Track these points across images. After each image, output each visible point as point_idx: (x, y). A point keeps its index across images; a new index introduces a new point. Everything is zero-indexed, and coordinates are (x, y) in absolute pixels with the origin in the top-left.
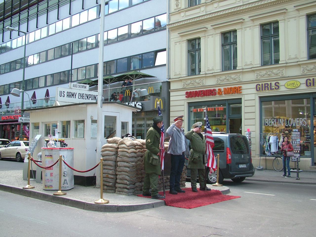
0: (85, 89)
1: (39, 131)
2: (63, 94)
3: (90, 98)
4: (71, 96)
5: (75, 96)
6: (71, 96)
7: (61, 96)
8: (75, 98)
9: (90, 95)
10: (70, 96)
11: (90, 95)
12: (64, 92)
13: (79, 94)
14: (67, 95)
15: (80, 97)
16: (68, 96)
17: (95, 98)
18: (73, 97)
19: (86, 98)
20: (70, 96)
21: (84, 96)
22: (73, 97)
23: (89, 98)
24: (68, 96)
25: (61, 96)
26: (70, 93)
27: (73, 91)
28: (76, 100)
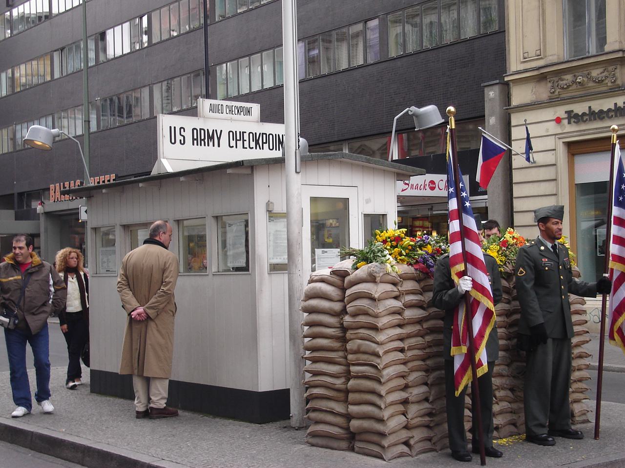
0: (247, 117)
1: (114, 252)
3: (266, 143)
4: (206, 140)
5: (219, 139)
7: (173, 141)
8: (219, 146)
9: (266, 134)
10: (203, 142)
12: (182, 130)
13: (231, 133)
14: (193, 139)
15: (233, 143)
16: (195, 142)
18: (211, 144)
19: (253, 144)
20: (201, 140)
21: (246, 137)
22: (211, 144)
23: (263, 143)
24: (197, 139)
25: (173, 141)
26: (202, 131)
27: (210, 126)
28: (222, 154)
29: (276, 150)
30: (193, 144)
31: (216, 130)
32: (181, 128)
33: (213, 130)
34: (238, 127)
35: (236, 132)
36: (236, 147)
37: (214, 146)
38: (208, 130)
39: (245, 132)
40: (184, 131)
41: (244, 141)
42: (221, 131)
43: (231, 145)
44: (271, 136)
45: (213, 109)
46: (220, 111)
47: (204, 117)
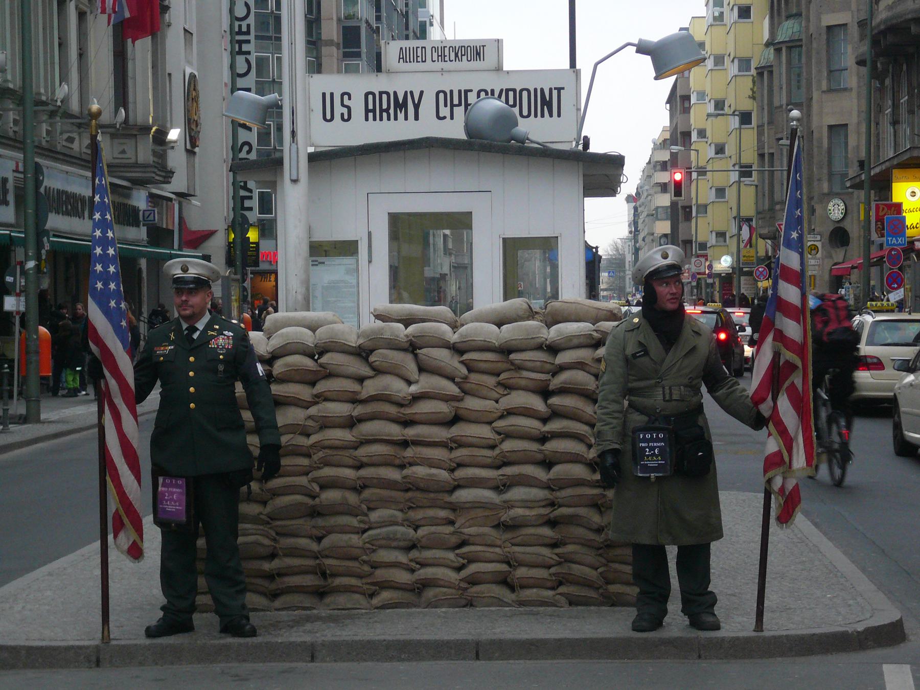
2: (343, 105)
4: (392, 111)
5: (417, 107)
6: (387, 110)
7: (328, 117)
8: (417, 118)
9: (514, 90)
10: (385, 115)
11: (507, 90)
12: (346, 97)
13: (441, 96)
14: (367, 111)
16: (371, 115)
17: (547, 103)
18: (401, 116)
20: (382, 111)
22: (401, 116)
24: (374, 111)
25: (328, 117)
26: (385, 97)
29: (536, 116)
30: (367, 119)
31: (411, 93)
32: (343, 95)
33: (406, 92)
34: (454, 84)
35: (451, 92)
36: (452, 118)
37: (406, 119)
38: (395, 93)
39: (471, 91)
40: (350, 99)
41: (467, 105)
42: (422, 93)
43: (441, 115)
44: (525, 94)
45: (403, 57)
46: (420, 59)
47: (388, 72)
